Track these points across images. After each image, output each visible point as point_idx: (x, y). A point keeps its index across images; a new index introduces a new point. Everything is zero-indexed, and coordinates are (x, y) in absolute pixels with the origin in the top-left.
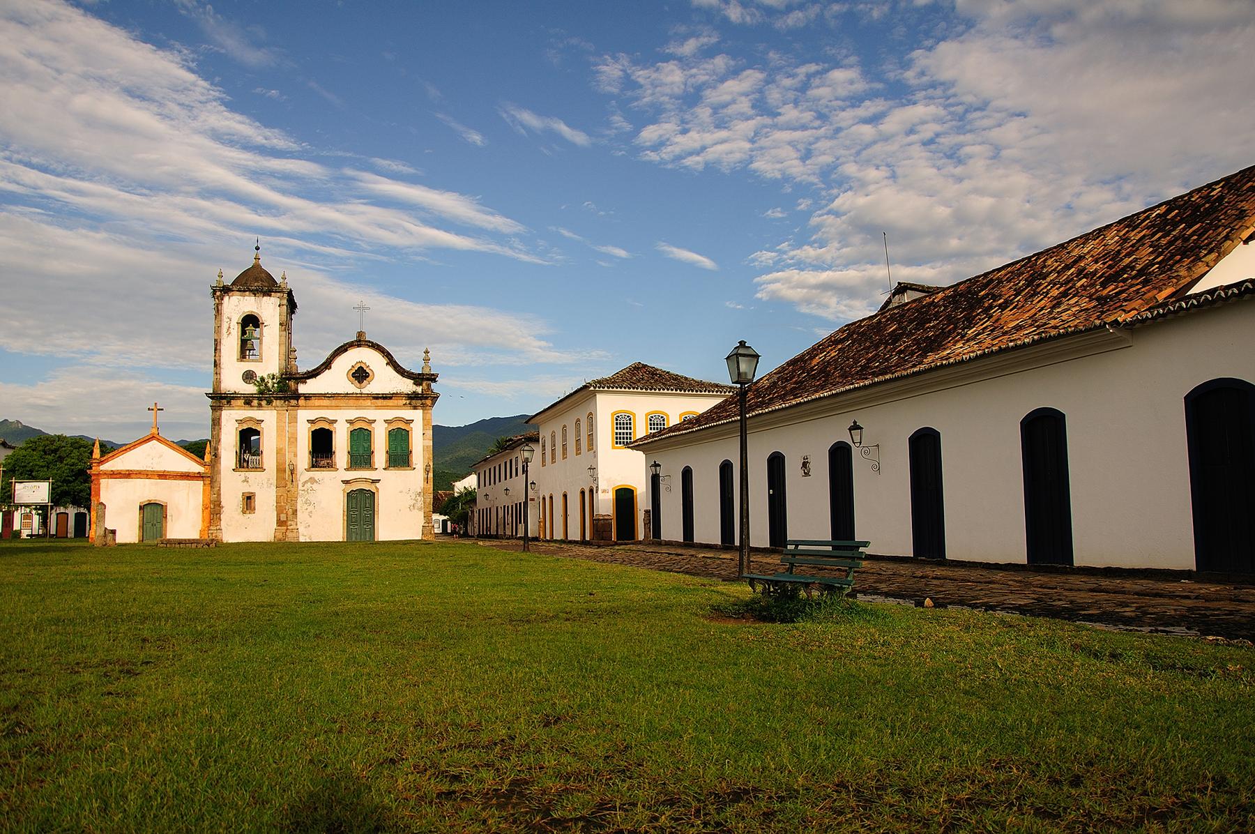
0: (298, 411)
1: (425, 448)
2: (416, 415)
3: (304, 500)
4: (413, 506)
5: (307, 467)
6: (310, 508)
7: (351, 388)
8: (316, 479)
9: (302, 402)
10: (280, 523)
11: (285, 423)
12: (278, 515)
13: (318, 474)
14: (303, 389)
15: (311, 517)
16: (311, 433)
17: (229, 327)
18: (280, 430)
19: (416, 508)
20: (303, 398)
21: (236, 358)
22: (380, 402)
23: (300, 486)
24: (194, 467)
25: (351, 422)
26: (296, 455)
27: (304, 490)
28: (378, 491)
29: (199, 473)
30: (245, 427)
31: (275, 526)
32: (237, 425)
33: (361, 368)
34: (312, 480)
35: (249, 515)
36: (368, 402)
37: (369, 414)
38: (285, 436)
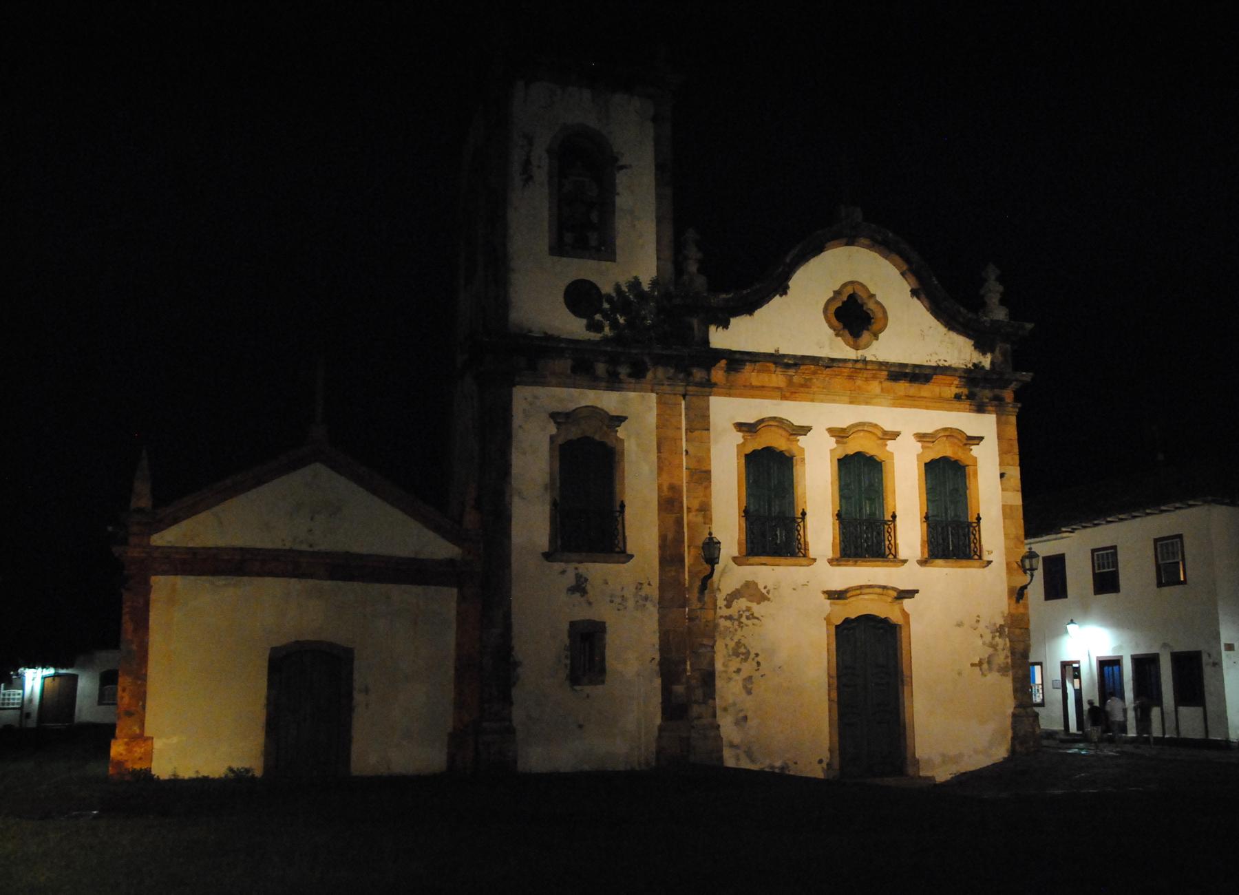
0: (710, 397)
1: (1008, 511)
2: (984, 425)
3: (732, 644)
4: (989, 662)
5: (736, 554)
6: (748, 668)
7: (841, 349)
8: (761, 587)
9: (718, 374)
10: (674, 710)
11: (680, 429)
12: (666, 691)
13: (767, 573)
14: (719, 339)
15: (749, 692)
16: (743, 461)
17: (527, 163)
18: (664, 444)
19: (995, 667)
20: (723, 363)
21: (546, 248)
22: (902, 387)
23: (721, 602)
24: (440, 549)
25: (840, 434)
26: (708, 519)
27: (730, 618)
28: (908, 623)
29: (451, 562)
30: (574, 433)
31: (658, 721)
32: (552, 429)
33: (852, 297)
34: (750, 591)
35: (588, 689)
36: (875, 387)
37: (884, 415)
38: (680, 465)
